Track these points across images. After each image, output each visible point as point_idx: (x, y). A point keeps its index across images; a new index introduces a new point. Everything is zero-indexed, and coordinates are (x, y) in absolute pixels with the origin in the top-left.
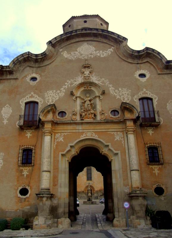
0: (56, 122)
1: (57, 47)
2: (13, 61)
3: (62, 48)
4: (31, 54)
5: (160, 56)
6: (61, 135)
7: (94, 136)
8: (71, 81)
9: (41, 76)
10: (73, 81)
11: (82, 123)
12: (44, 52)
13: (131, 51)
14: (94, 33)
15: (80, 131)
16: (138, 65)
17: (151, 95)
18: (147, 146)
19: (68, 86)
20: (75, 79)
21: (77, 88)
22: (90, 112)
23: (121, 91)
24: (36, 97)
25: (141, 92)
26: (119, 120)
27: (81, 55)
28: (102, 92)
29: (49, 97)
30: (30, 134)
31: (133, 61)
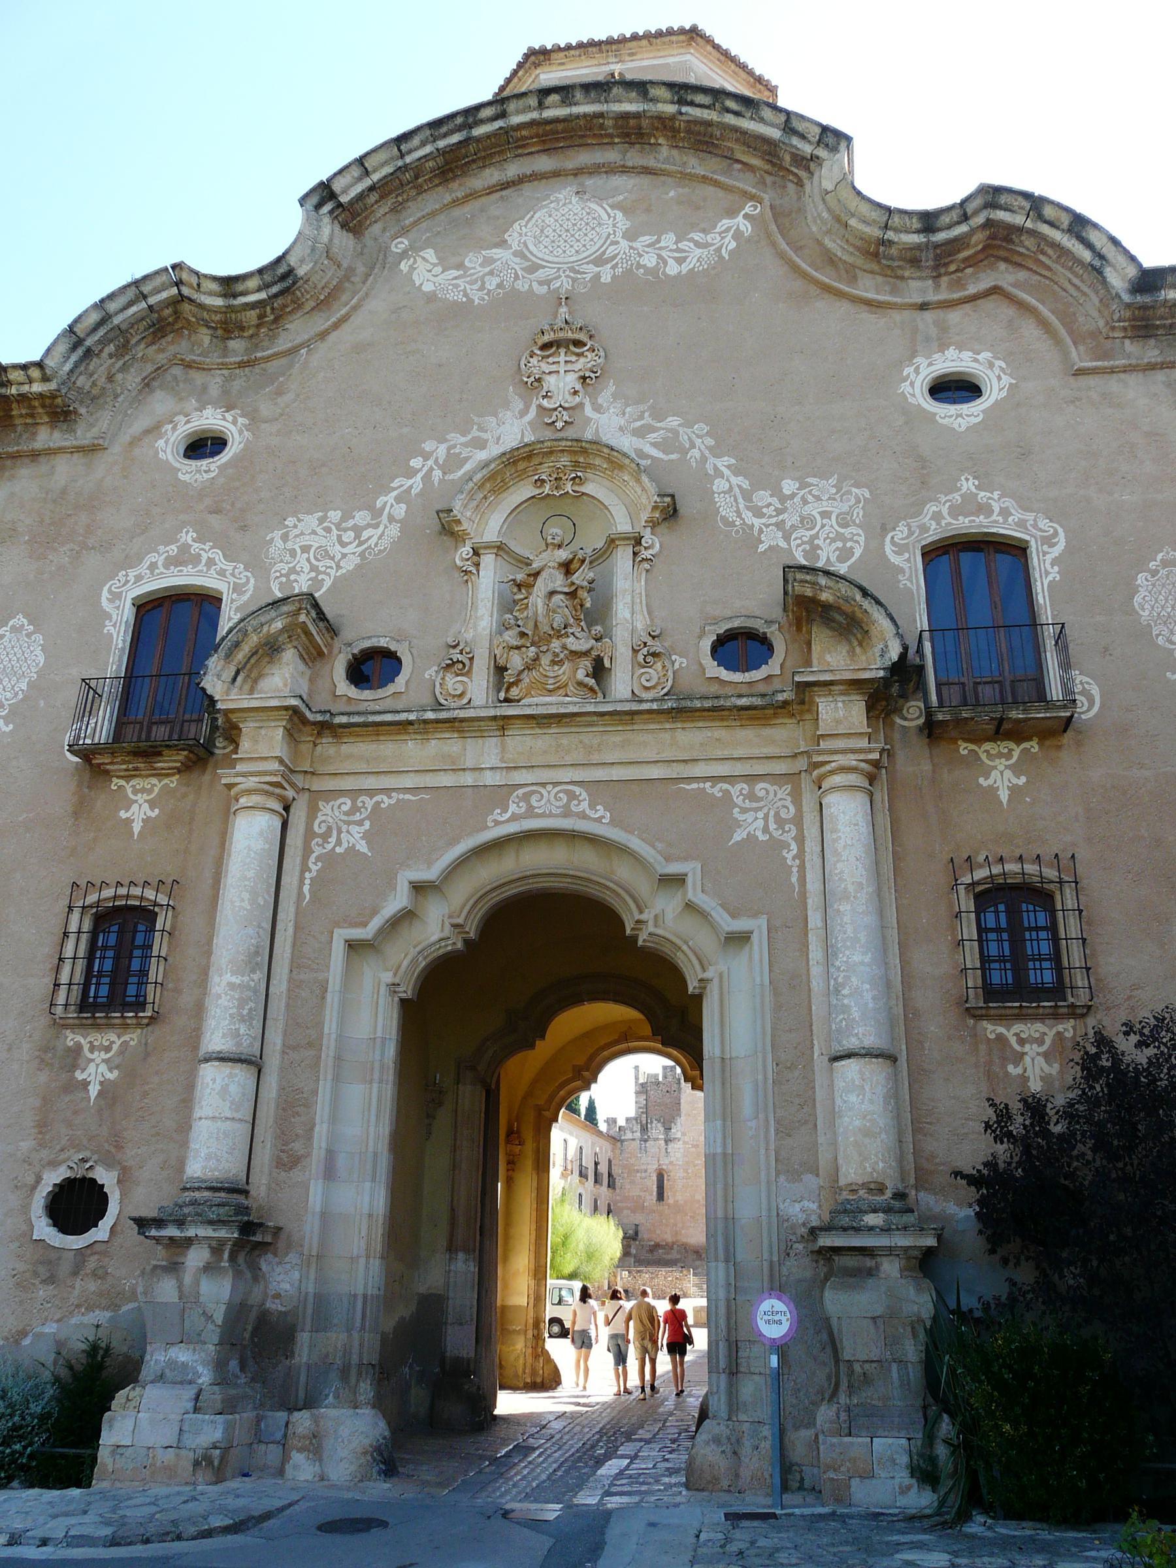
0: (319, 718)
1: (376, 229)
2: (71, 329)
3: (404, 231)
4: (194, 280)
5: (1089, 246)
6: (354, 809)
7: (583, 816)
8: (454, 446)
9: (254, 419)
10: (465, 445)
11: (503, 724)
12: (279, 260)
14: (626, 116)
15: (490, 779)
16: (928, 316)
17: (1017, 515)
18: (967, 879)
19: (427, 477)
20: (475, 433)
21: (481, 487)
22: (564, 647)
23: (793, 495)
24: (211, 562)
25: (943, 499)
26: (763, 696)
27: (533, 268)
28: (655, 508)
29: (293, 553)
30: (152, 808)
31: (894, 291)
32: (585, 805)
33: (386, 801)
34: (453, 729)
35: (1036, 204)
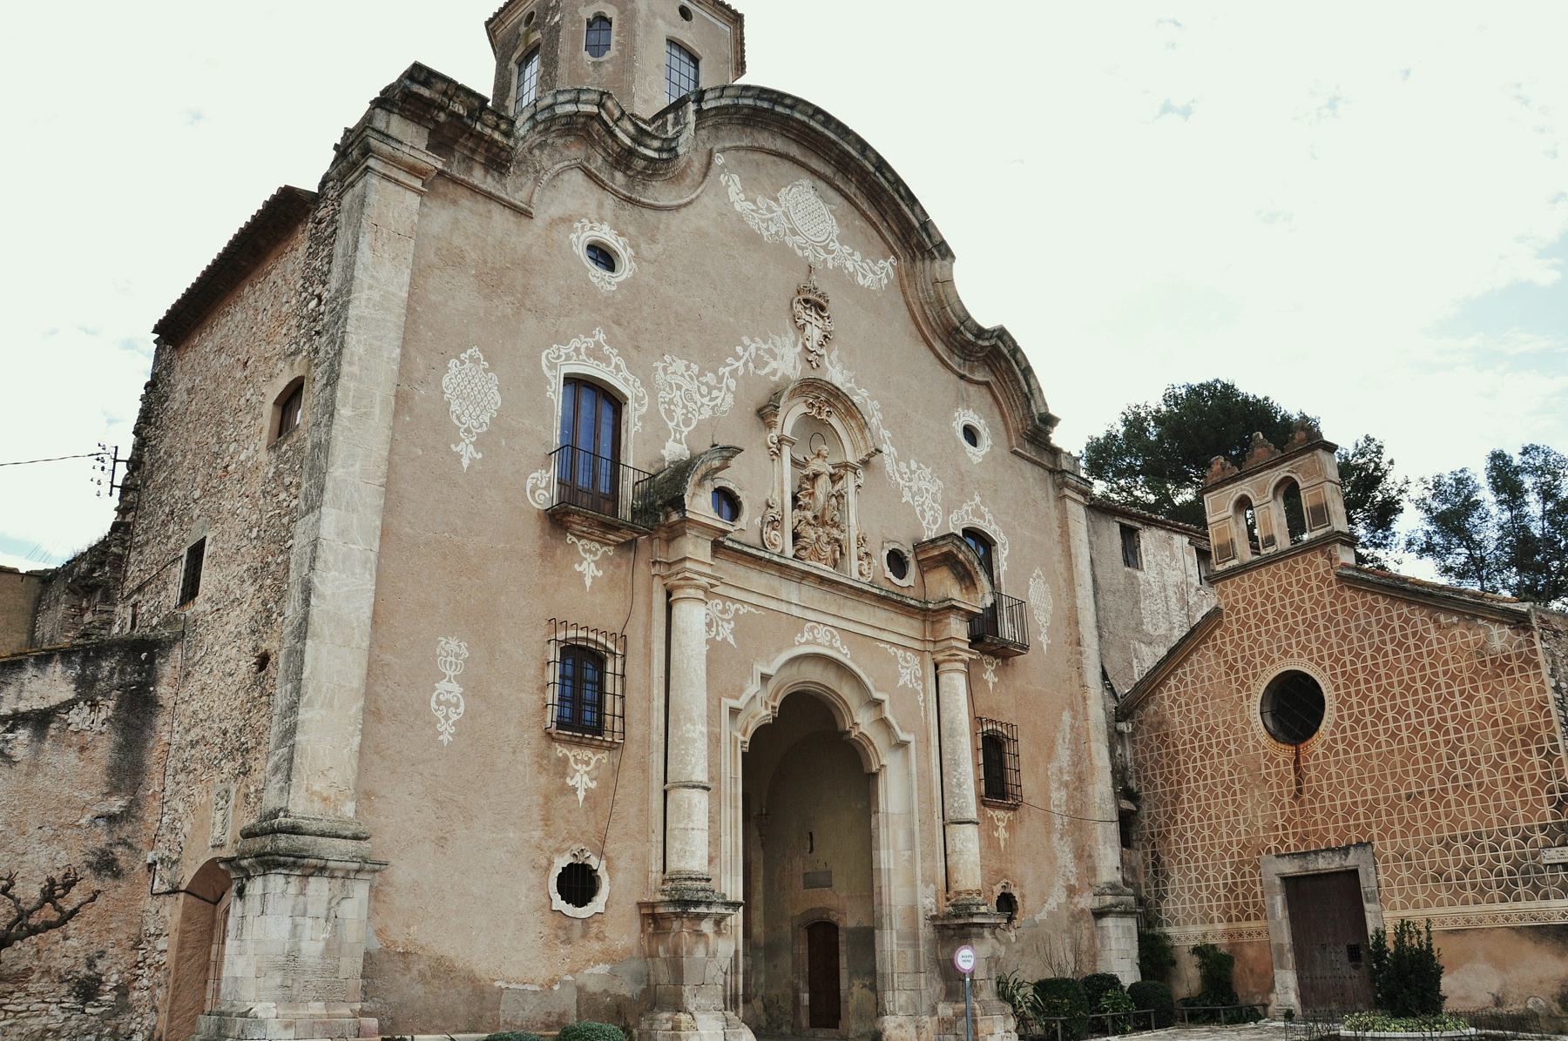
6: (724, 611)
13: (961, 314)
15: (796, 611)
17: (994, 526)
19: (746, 364)
32: (838, 643)
33: (744, 610)
34: (778, 570)
35: (1015, 350)
